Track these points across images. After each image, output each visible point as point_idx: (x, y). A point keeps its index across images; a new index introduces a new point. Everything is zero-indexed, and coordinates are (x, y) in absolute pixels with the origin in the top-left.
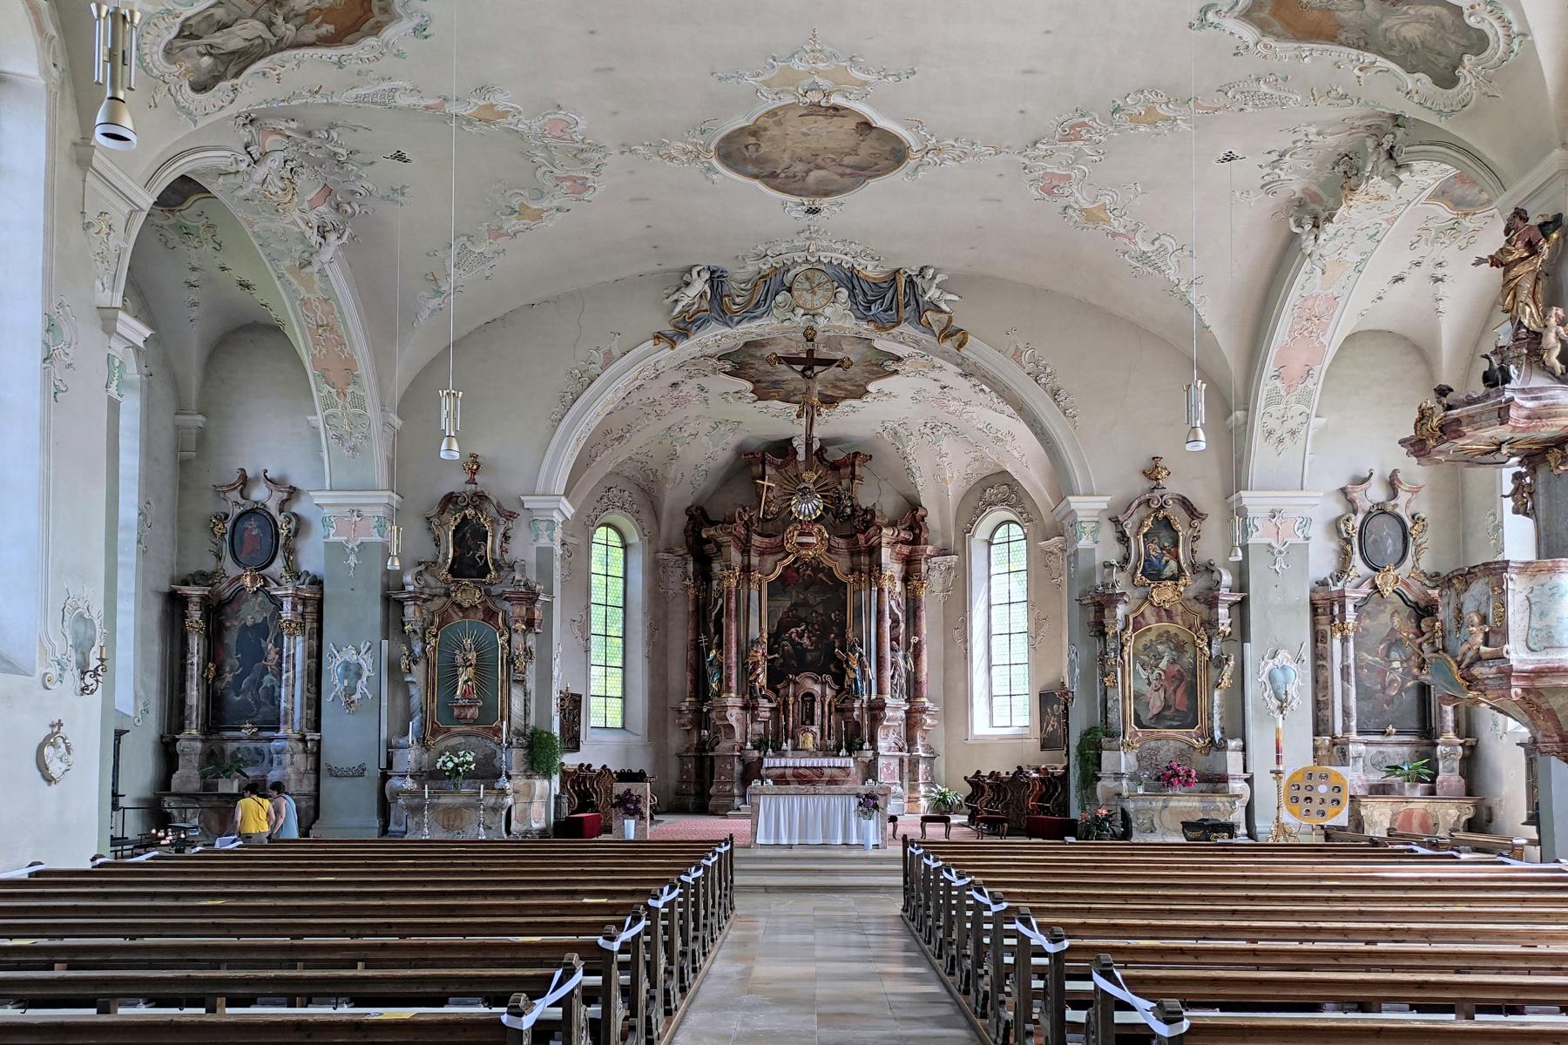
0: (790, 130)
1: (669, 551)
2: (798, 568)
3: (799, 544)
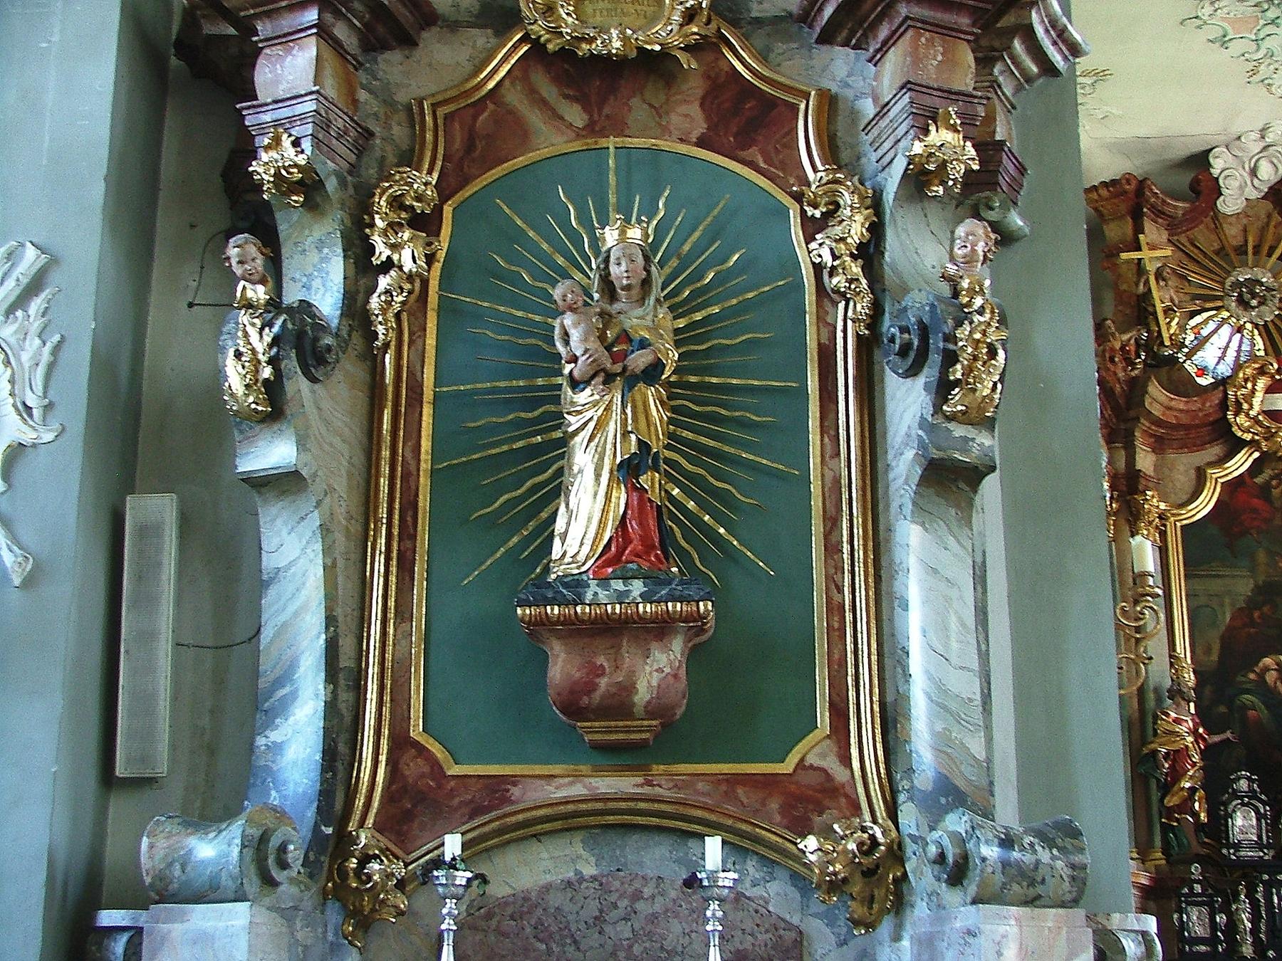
2: (1266, 487)
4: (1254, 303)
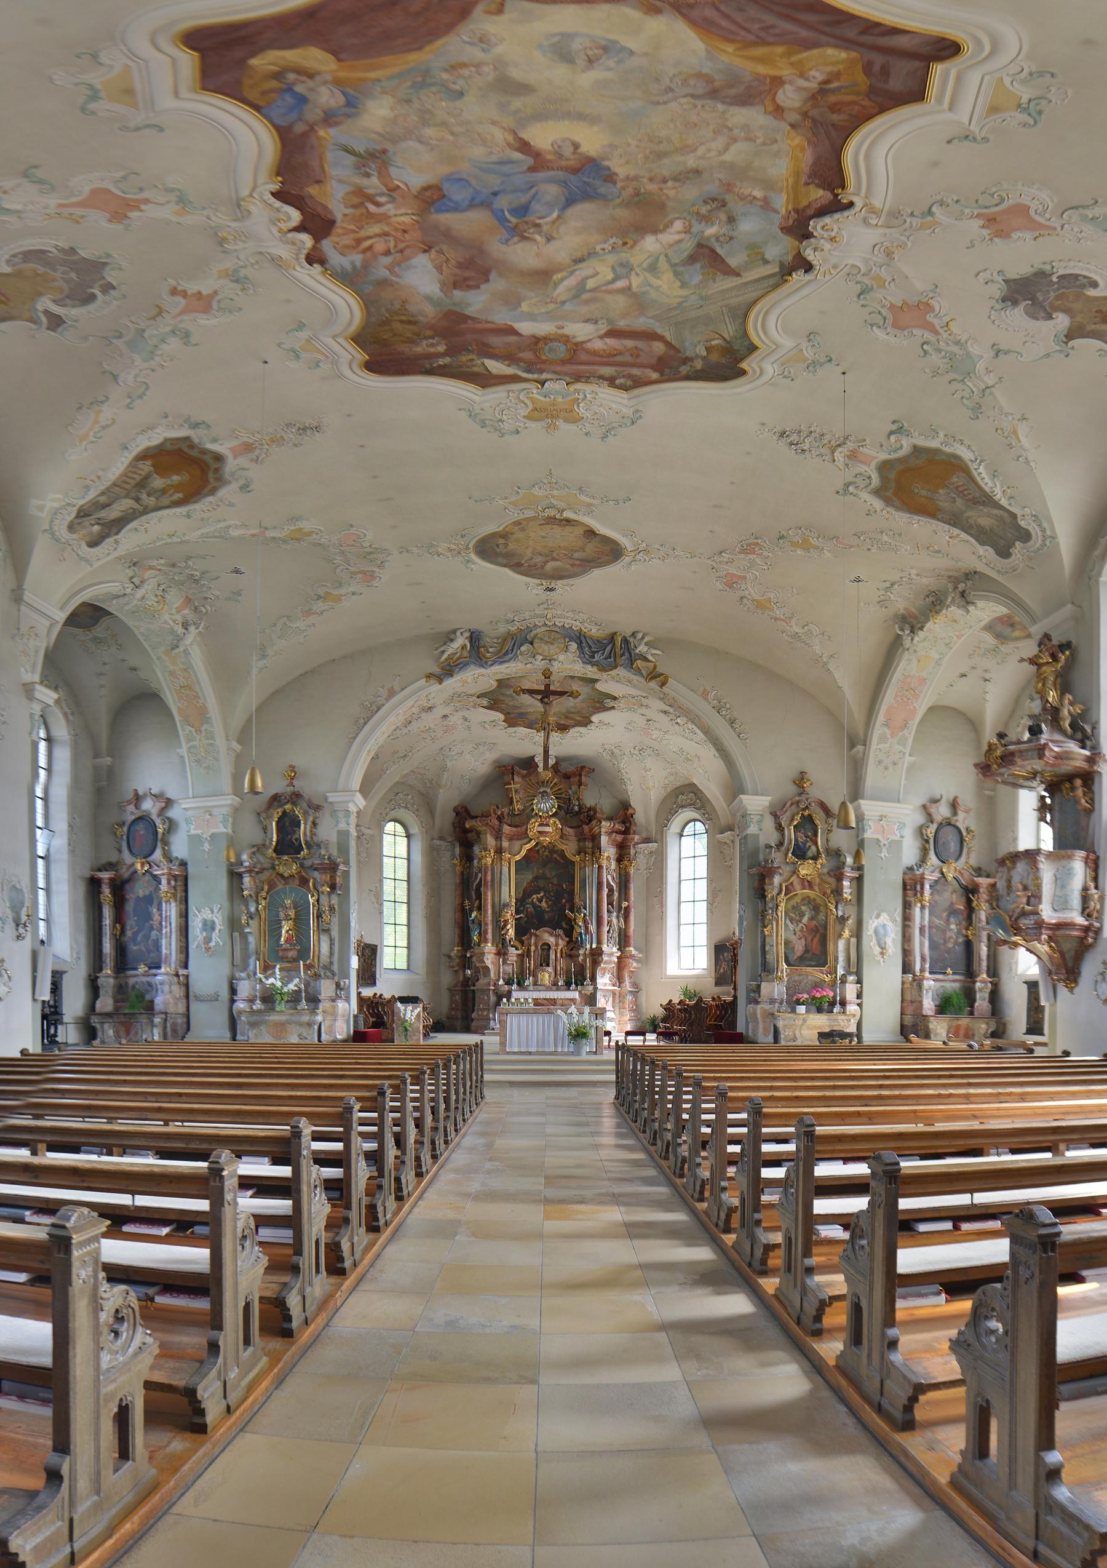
0: (532, 534)
1: (441, 838)
3: (540, 832)
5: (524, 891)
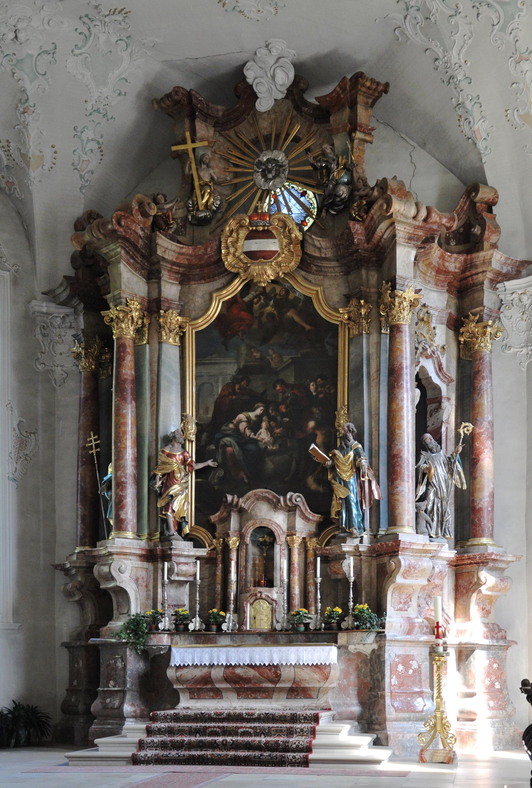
2: (251, 302)
3: (252, 255)
4: (270, 176)
5: (218, 404)
